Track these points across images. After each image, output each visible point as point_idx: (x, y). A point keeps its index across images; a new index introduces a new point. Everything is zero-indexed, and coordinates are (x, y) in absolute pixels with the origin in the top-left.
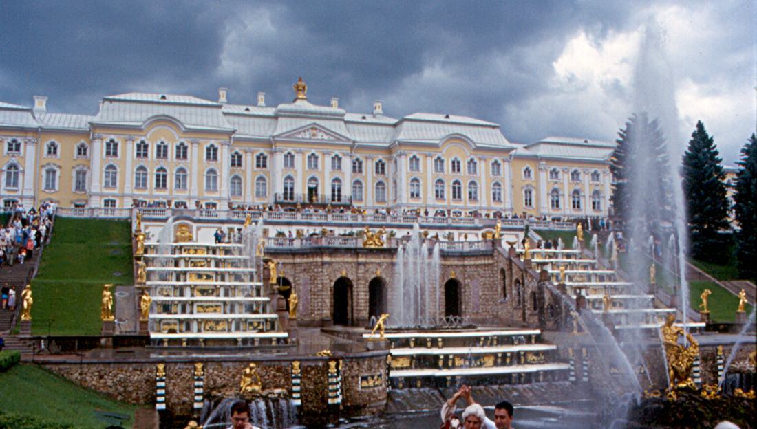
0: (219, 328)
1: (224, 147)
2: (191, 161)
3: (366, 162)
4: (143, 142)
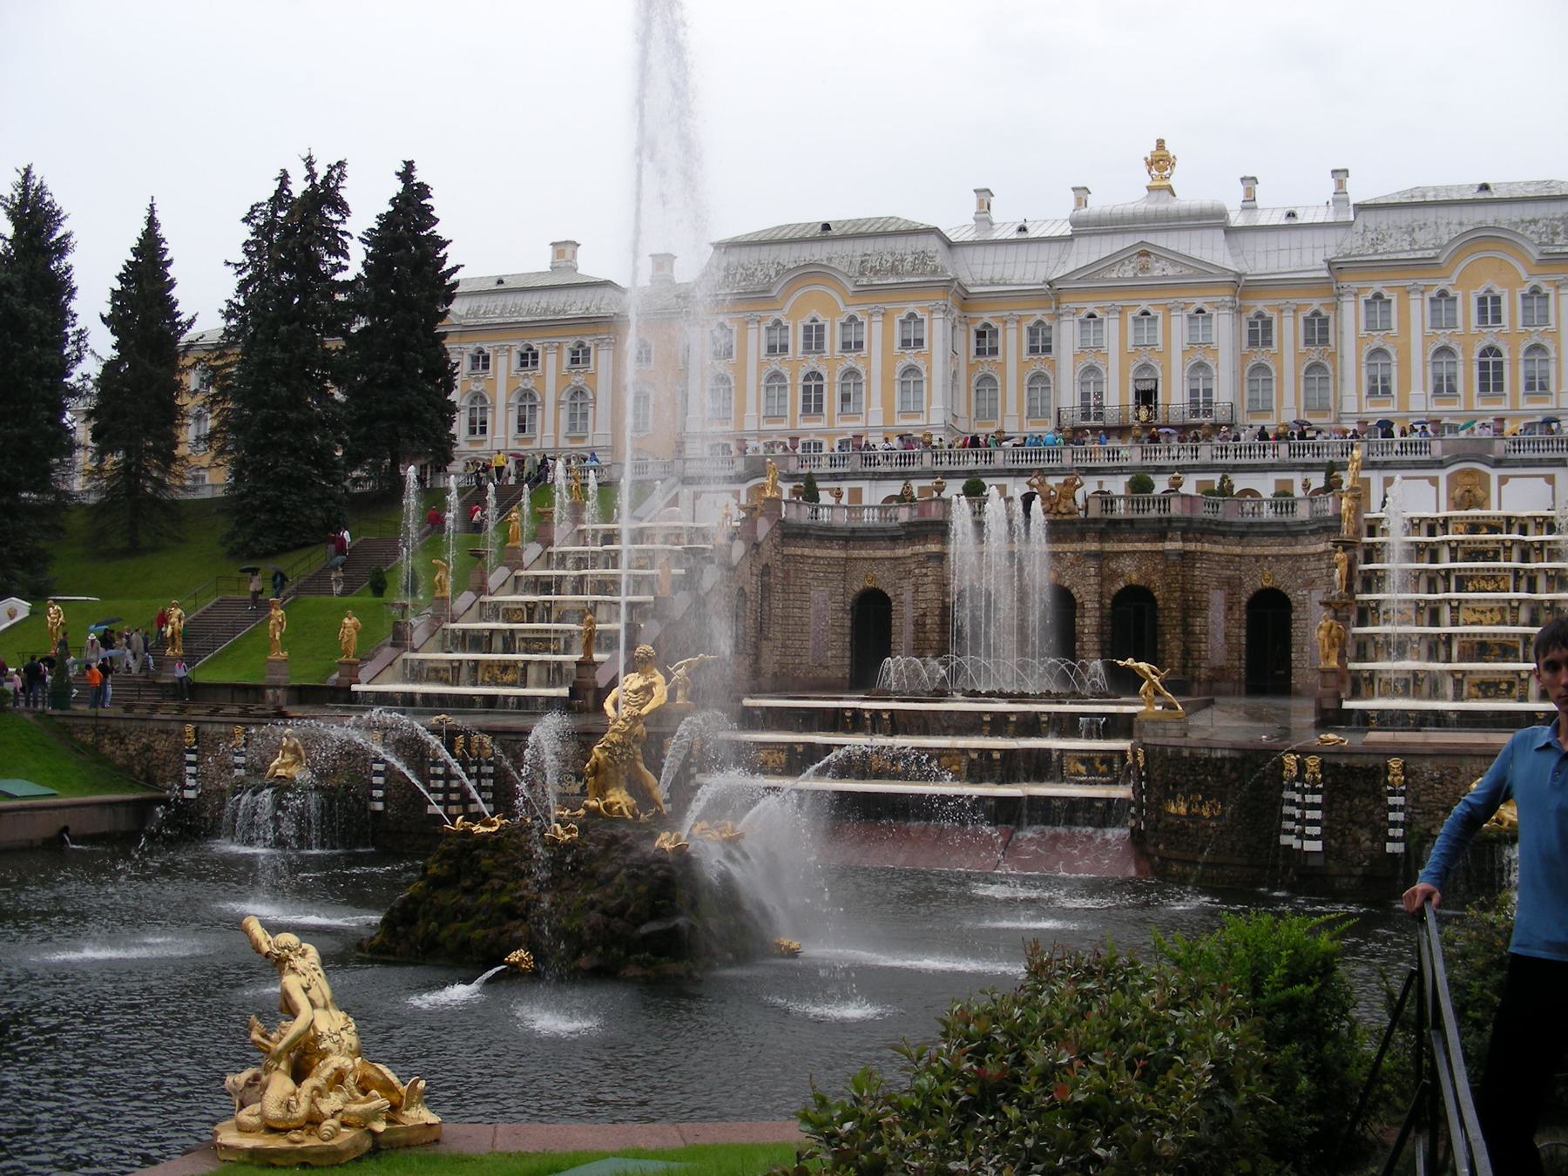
0: (509, 677)
1: (935, 316)
2: (869, 353)
3: (1280, 319)
4: (778, 323)
